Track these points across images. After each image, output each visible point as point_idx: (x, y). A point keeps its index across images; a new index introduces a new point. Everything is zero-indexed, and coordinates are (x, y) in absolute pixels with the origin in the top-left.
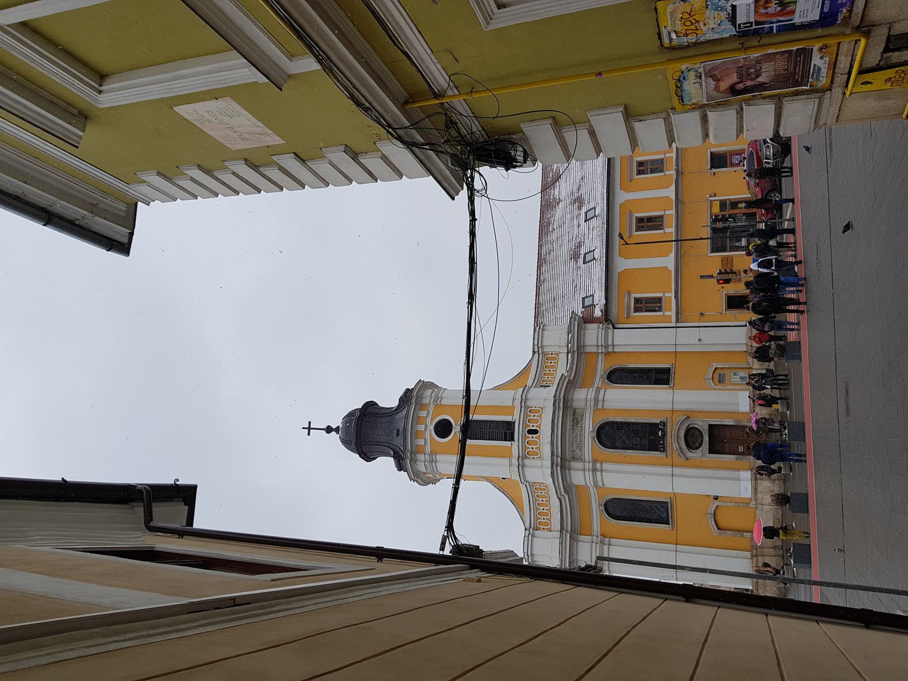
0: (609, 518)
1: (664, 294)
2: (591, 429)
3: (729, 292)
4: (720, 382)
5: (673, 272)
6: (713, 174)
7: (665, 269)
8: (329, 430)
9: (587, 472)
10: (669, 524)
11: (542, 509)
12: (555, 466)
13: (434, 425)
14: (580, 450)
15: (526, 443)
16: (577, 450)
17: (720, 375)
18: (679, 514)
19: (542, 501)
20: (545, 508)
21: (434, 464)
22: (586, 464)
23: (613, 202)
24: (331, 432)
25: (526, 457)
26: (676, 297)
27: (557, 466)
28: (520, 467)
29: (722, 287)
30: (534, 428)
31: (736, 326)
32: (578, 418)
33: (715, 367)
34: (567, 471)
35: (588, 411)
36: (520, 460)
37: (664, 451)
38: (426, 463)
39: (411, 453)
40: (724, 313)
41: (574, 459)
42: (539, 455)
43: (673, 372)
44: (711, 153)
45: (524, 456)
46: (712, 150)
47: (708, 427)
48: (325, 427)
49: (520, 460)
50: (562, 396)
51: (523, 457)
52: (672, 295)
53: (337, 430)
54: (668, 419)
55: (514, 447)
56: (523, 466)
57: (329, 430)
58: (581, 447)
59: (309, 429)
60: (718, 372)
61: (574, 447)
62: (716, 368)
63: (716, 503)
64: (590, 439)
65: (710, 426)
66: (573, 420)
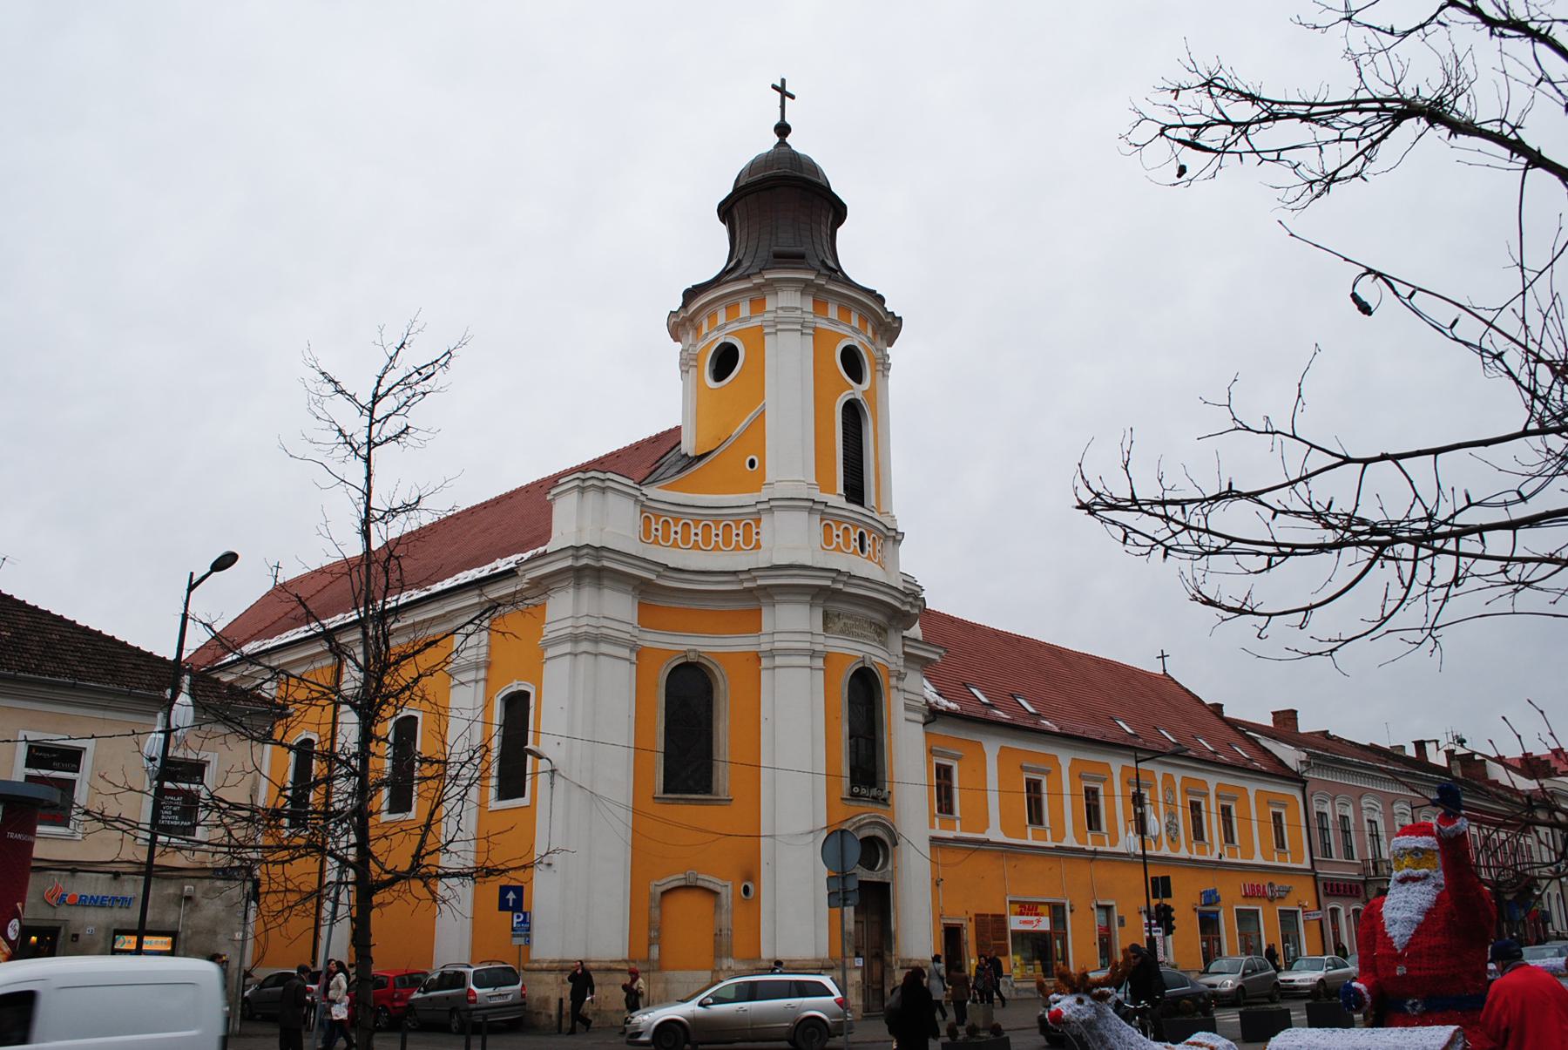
0: (669, 670)
1: (958, 818)
2: (874, 658)
3: (965, 931)
7: (985, 825)
8: (783, 130)
9: (808, 637)
10: (665, 791)
11: (676, 529)
12: (834, 575)
13: (859, 348)
14: (842, 632)
15: (667, 518)
16: (842, 625)
18: (689, 812)
19: (737, 535)
20: (679, 536)
21: (799, 327)
22: (821, 639)
24: (778, 136)
25: (822, 520)
26: (956, 840)
27: (834, 580)
28: (810, 504)
29: (970, 919)
30: (867, 548)
34: (809, 598)
35: (885, 656)
36: (822, 507)
37: (852, 794)
38: (800, 312)
39: (820, 288)
40: (942, 921)
41: (826, 617)
42: (745, 548)
44: (1112, 906)
45: (825, 516)
46: (1115, 908)
48: (787, 120)
49: (822, 507)
51: (823, 512)
52: (958, 833)
53: (782, 143)
55: (837, 499)
56: (811, 510)
57: (783, 130)
58: (846, 632)
59: (781, 90)
61: (846, 621)
63: (728, 891)
64: (861, 655)
65: (888, 884)
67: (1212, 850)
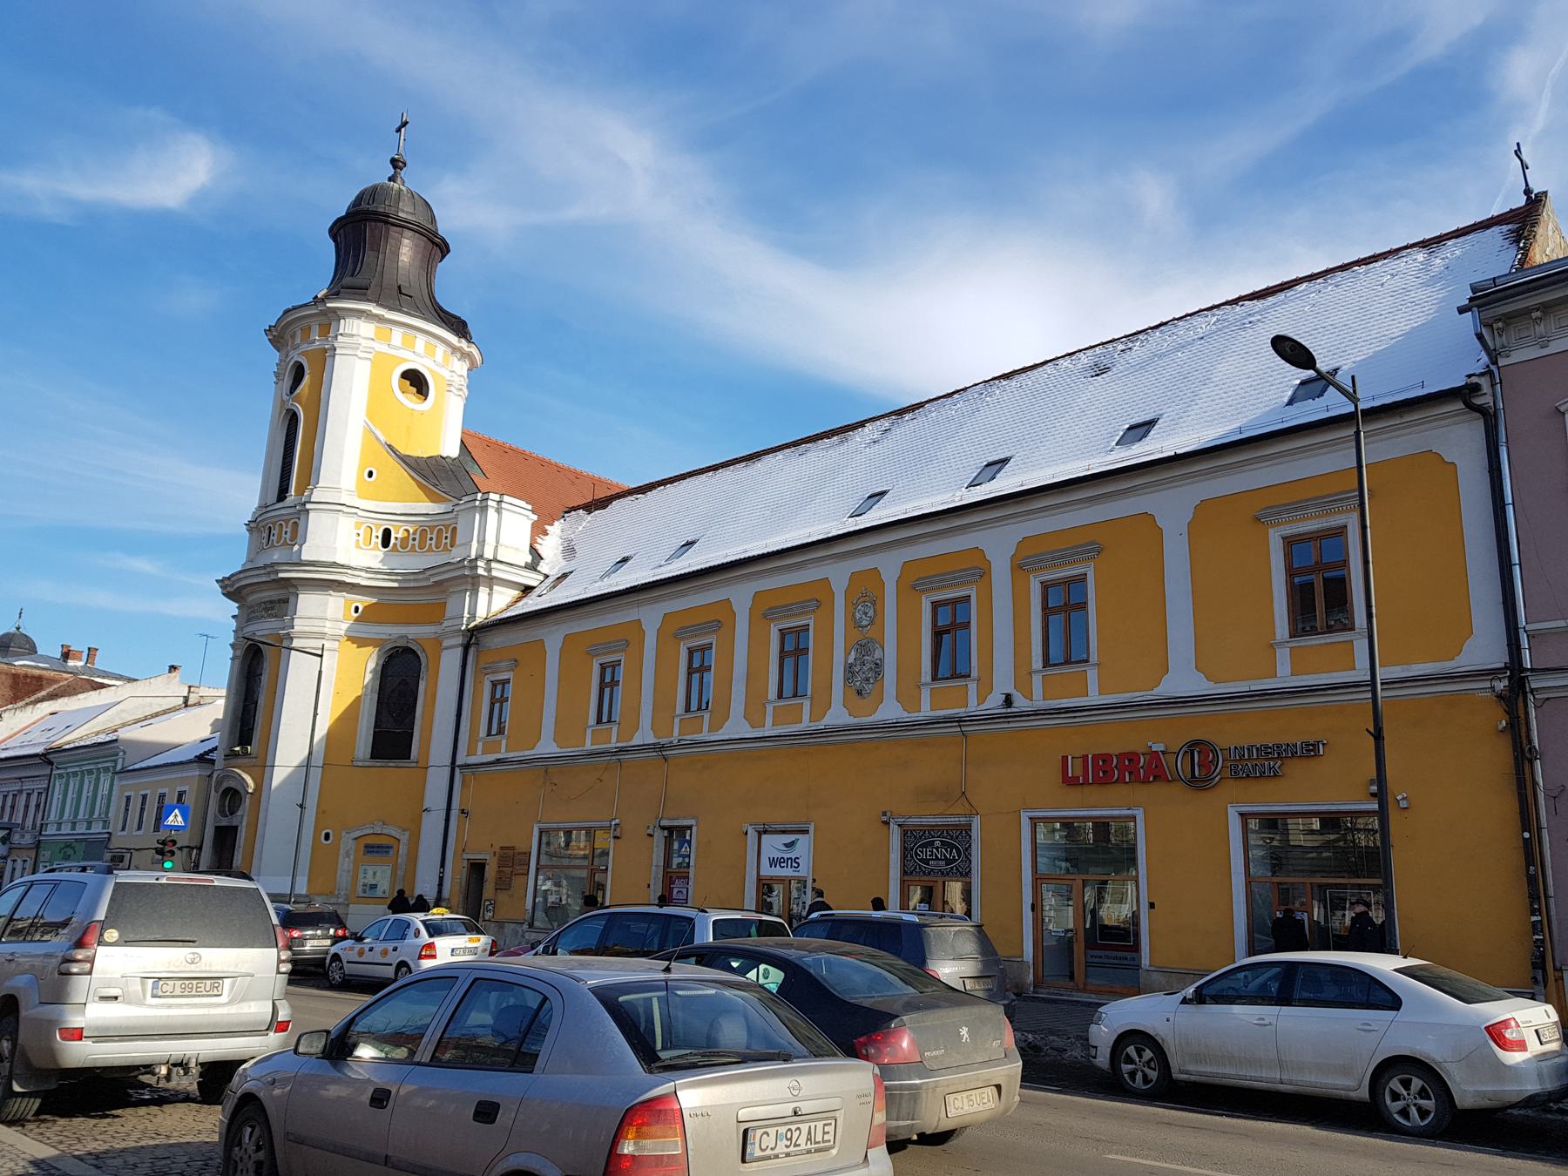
4: (366, 846)
5: (532, 752)
6: (650, 832)
17: (388, 847)
23: (639, 604)
26: (498, 761)
29: (495, 853)
31: (441, 879)
32: (273, 608)
33: (401, 838)
40: (465, 856)
43: (400, 765)
47: (234, 824)
50: (244, 583)
54: (254, 760)
60: (396, 842)
62: (399, 840)
65: (236, 827)
66: (271, 602)
67: (986, 687)
